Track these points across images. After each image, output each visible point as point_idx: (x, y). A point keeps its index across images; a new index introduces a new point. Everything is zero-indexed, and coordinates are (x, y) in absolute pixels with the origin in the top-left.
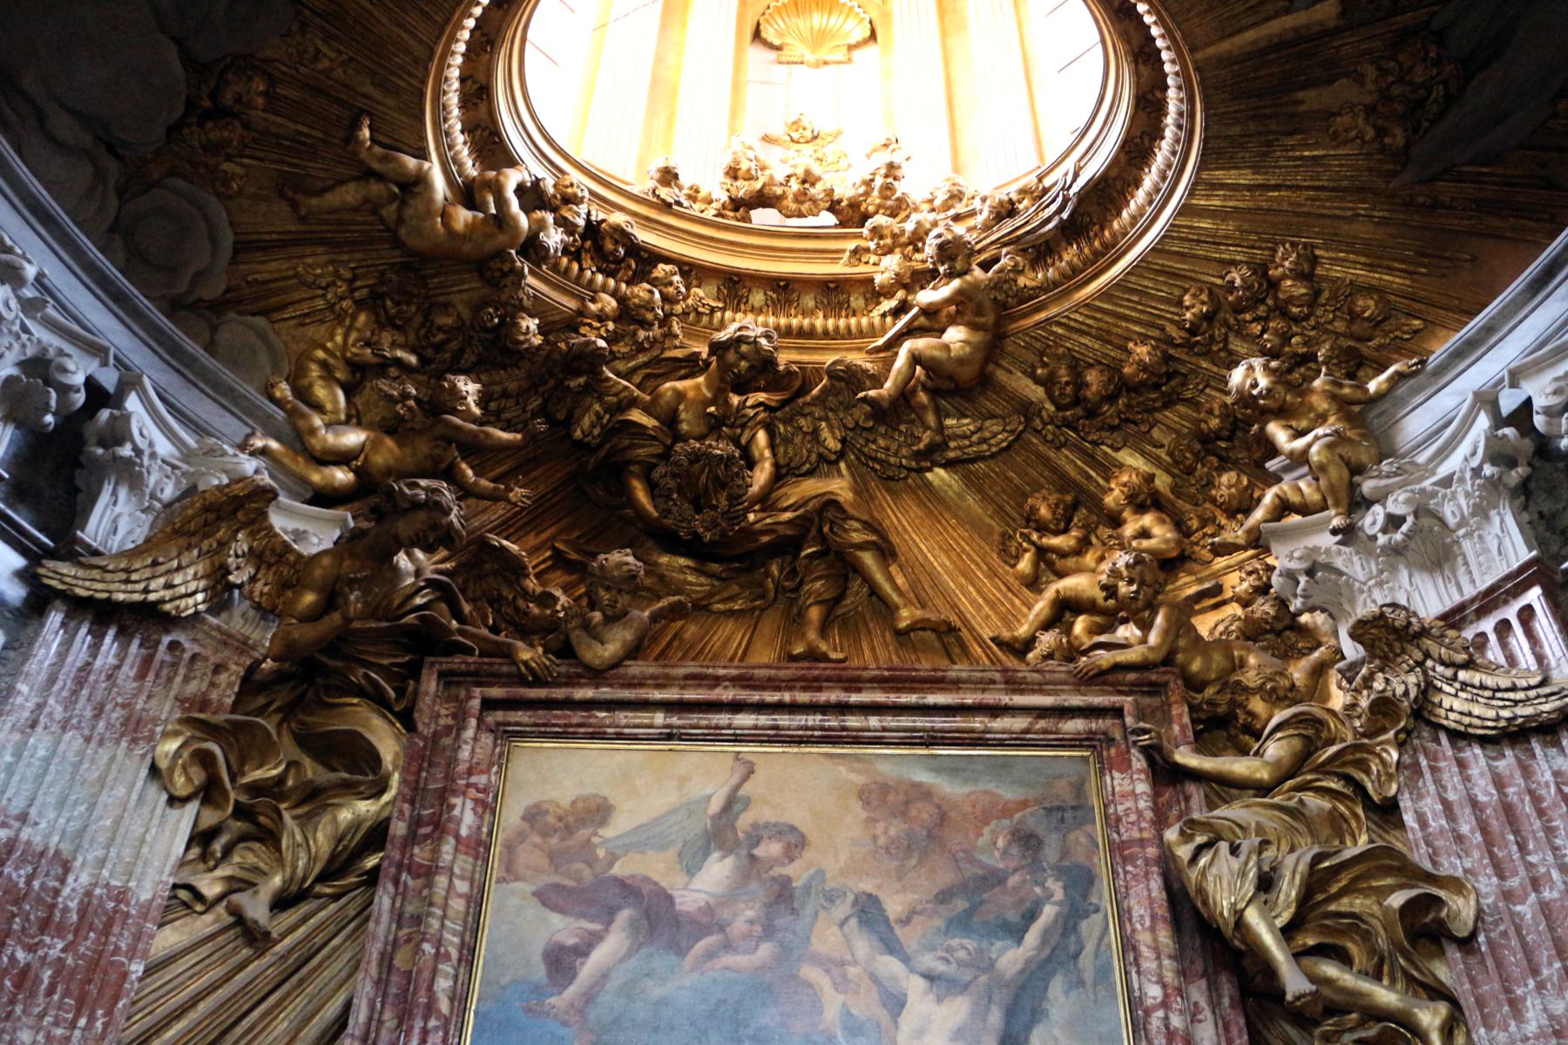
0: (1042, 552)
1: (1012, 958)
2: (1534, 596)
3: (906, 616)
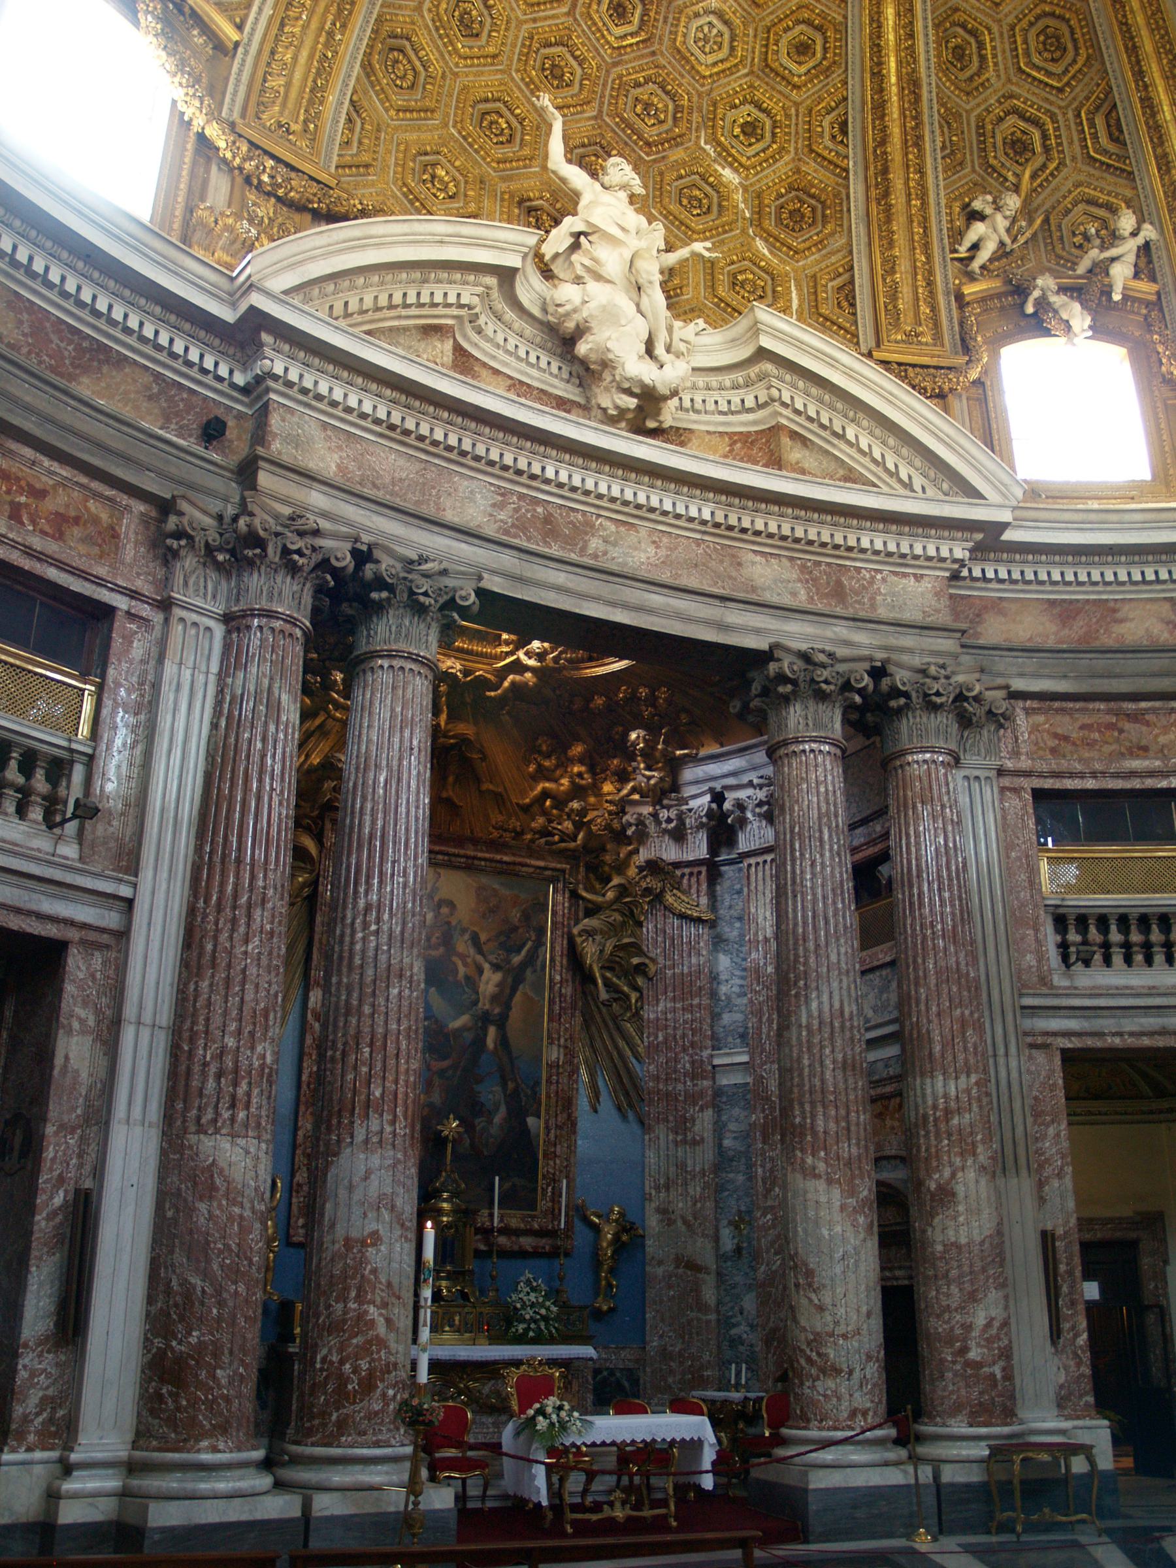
0: (540, 766)
1: (517, 959)
2: (704, 869)
3: (486, 786)
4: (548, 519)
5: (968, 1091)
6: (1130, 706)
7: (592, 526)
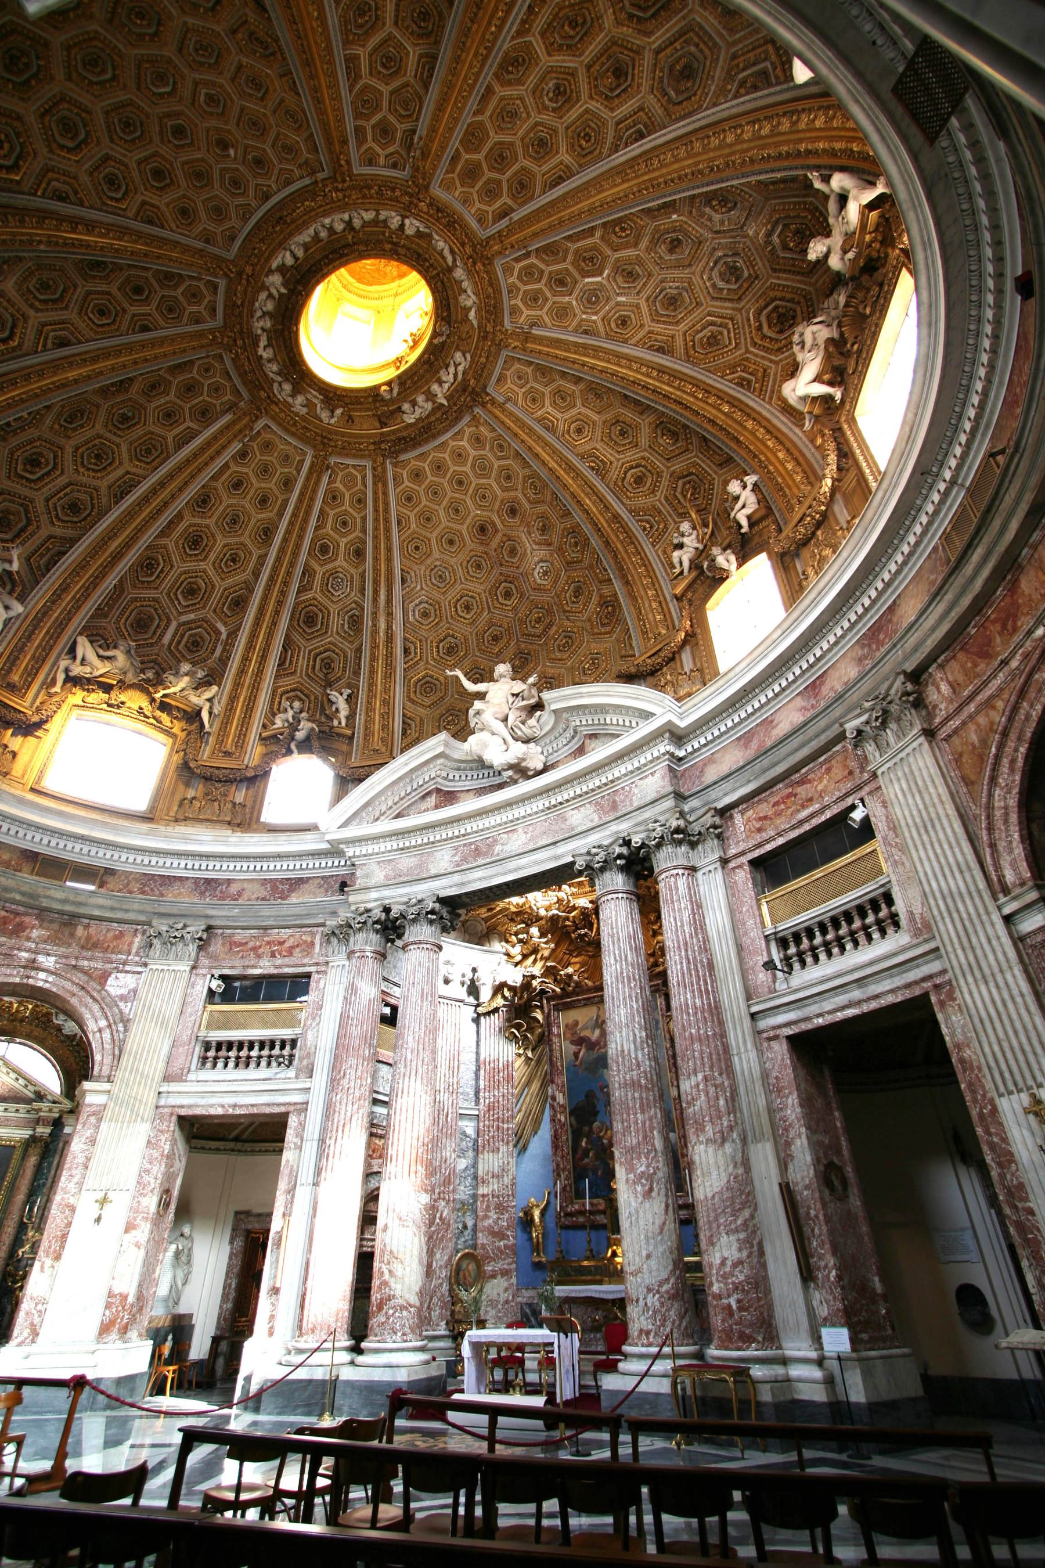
4: (476, 849)
5: (698, 1085)
6: (796, 777)
7: (496, 841)
